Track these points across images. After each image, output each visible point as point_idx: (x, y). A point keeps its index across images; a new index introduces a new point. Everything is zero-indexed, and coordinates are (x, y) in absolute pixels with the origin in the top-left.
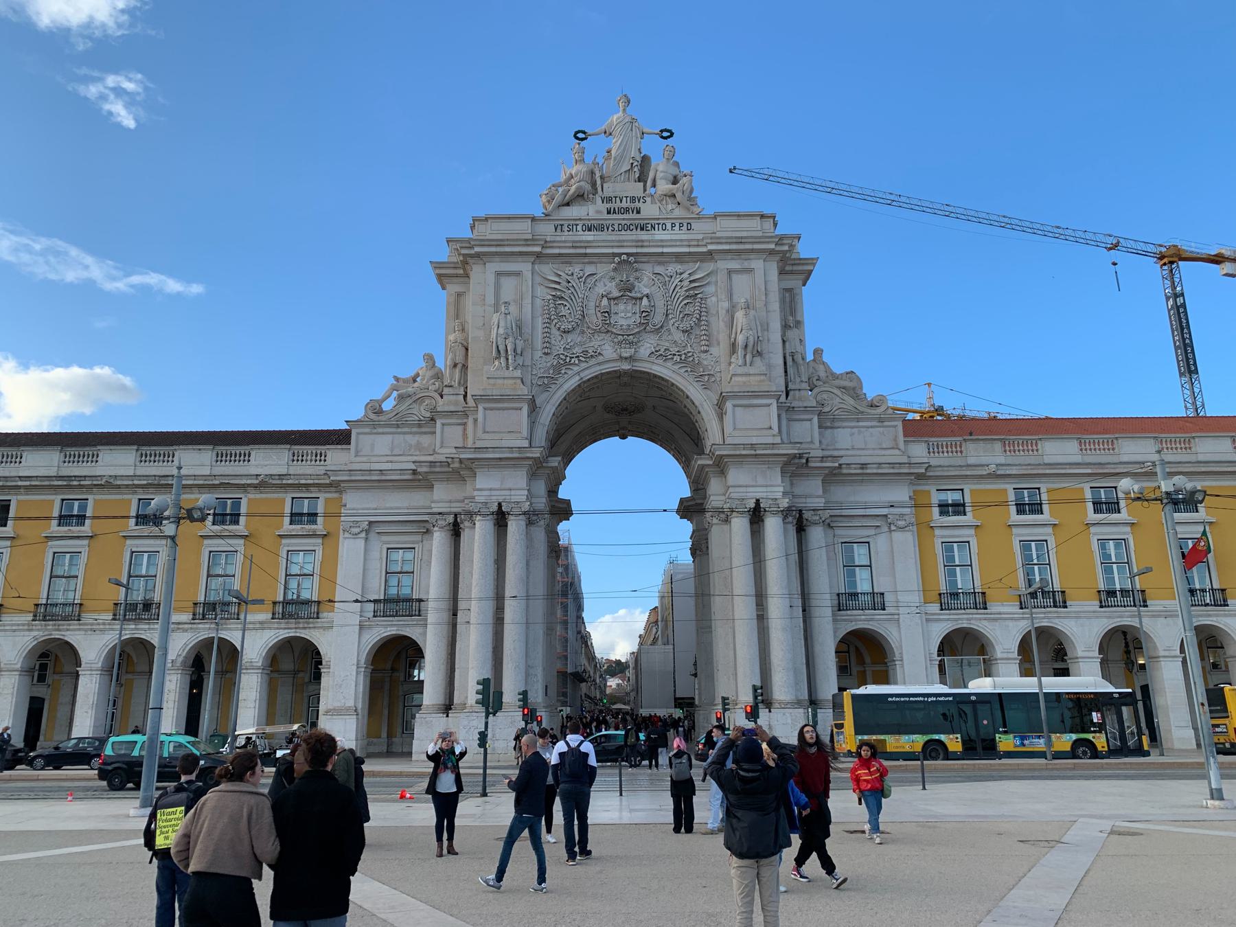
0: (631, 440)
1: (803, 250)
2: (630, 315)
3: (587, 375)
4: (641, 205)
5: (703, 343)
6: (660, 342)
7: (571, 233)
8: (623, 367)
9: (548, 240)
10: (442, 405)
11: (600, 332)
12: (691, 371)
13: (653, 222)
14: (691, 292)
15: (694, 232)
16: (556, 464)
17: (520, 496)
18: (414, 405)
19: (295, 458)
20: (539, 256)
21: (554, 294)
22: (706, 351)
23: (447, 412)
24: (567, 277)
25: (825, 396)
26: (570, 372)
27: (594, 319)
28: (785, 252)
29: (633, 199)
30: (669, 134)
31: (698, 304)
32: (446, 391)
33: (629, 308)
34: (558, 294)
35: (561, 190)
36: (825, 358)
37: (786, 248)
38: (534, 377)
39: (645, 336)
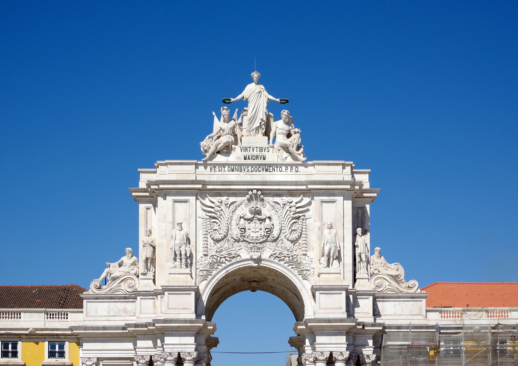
2: (257, 230)
3: (231, 269)
6: (276, 248)
7: (220, 173)
9: (206, 178)
12: (296, 267)
14: (297, 215)
15: (300, 173)
17: (192, 349)
18: (122, 284)
19: (50, 315)
20: (199, 189)
21: (210, 214)
22: (305, 255)
23: (144, 291)
24: (219, 204)
26: (220, 267)
27: (235, 232)
29: (261, 149)
31: (301, 223)
33: (257, 225)
34: (213, 215)
38: (197, 270)
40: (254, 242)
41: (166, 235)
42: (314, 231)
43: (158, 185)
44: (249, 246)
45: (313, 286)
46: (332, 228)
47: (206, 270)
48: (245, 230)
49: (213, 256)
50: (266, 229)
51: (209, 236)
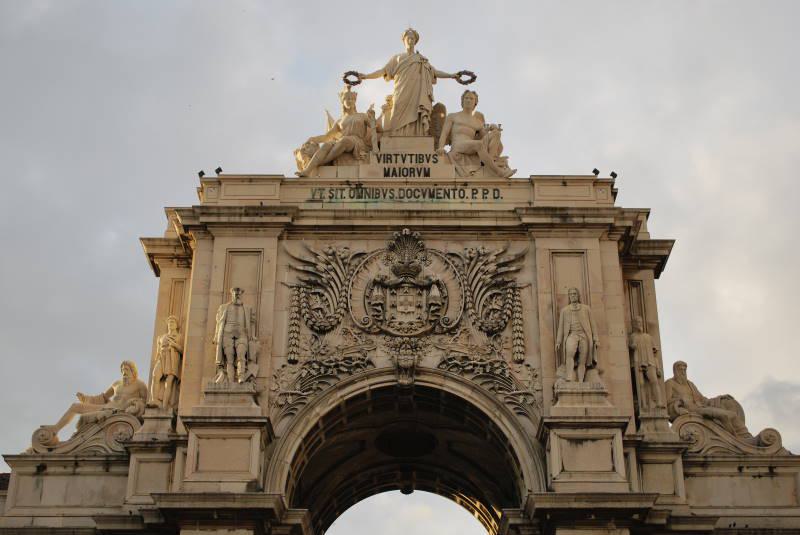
0: (418, 495)
1: (654, 230)
3: (349, 392)
4: (430, 165)
5: (517, 349)
7: (334, 200)
8: (400, 381)
9: (302, 207)
10: (141, 434)
11: (369, 333)
12: (500, 389)
13: (447, 187)
14: (500, 279)
16: (298, 521)
21: (307, 279)
22: (521, 362)
25: (692, 429)
26: (325, 388)
27: (359, 313)
28: (629, 229)
29: (420, 158)
30: (469, 78)
32: (149, 413)
33: (410, 299)
34: (313, 278)
35: (321, 145)
36: (690, 376)
37: (629, 223)
38: (273, 394)
39: (435, 339)
40: (403, 334)
41: (206, 321)
42: (538, 313)
43: (195, 218)
44: (392, 342)
45: (542, 419)
46: (579, 302)
47: (292, 394)
48: (383, 308)
49: (309, 363)
50: (432, 304)
51: (302, 324)
